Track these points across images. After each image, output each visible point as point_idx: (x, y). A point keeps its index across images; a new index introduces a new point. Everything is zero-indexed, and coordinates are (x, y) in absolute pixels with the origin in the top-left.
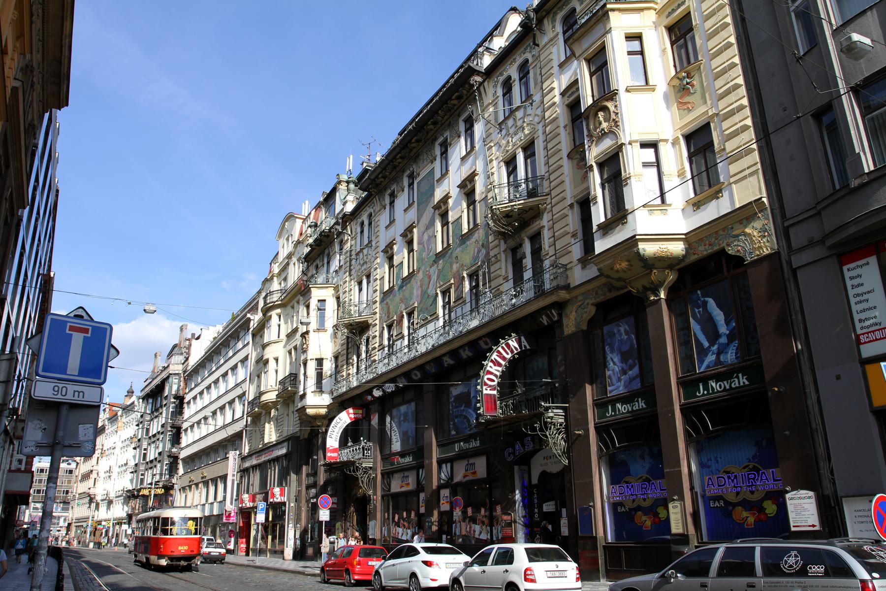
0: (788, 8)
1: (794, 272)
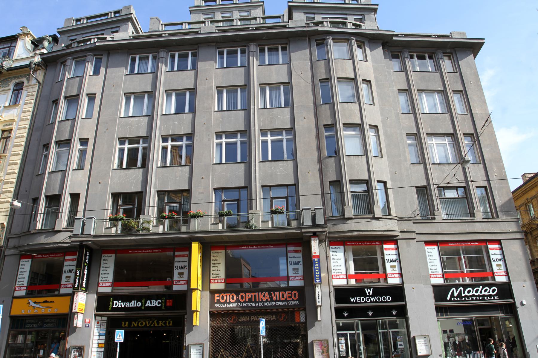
0: (43, 152)
1: (5, 256)
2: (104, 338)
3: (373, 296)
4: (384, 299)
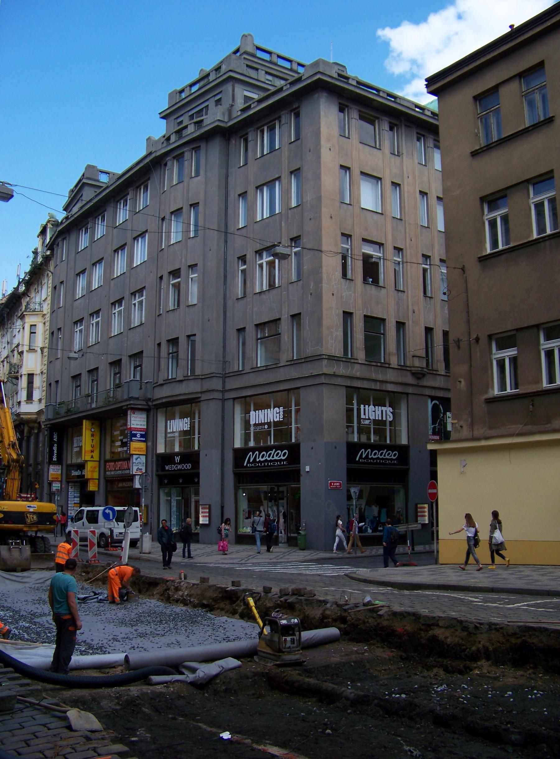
2: (78, 499)
3: (181, 462)
4: (186, 466)
